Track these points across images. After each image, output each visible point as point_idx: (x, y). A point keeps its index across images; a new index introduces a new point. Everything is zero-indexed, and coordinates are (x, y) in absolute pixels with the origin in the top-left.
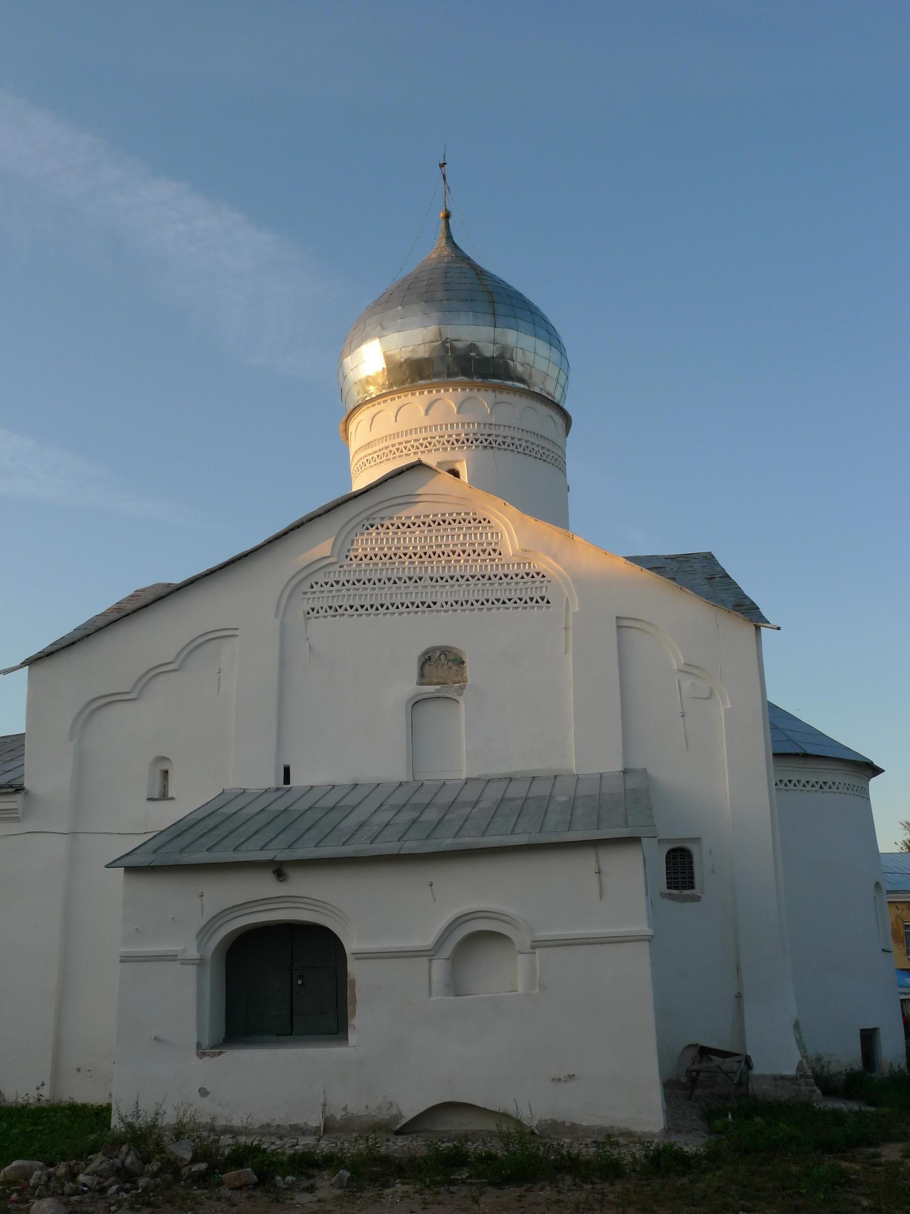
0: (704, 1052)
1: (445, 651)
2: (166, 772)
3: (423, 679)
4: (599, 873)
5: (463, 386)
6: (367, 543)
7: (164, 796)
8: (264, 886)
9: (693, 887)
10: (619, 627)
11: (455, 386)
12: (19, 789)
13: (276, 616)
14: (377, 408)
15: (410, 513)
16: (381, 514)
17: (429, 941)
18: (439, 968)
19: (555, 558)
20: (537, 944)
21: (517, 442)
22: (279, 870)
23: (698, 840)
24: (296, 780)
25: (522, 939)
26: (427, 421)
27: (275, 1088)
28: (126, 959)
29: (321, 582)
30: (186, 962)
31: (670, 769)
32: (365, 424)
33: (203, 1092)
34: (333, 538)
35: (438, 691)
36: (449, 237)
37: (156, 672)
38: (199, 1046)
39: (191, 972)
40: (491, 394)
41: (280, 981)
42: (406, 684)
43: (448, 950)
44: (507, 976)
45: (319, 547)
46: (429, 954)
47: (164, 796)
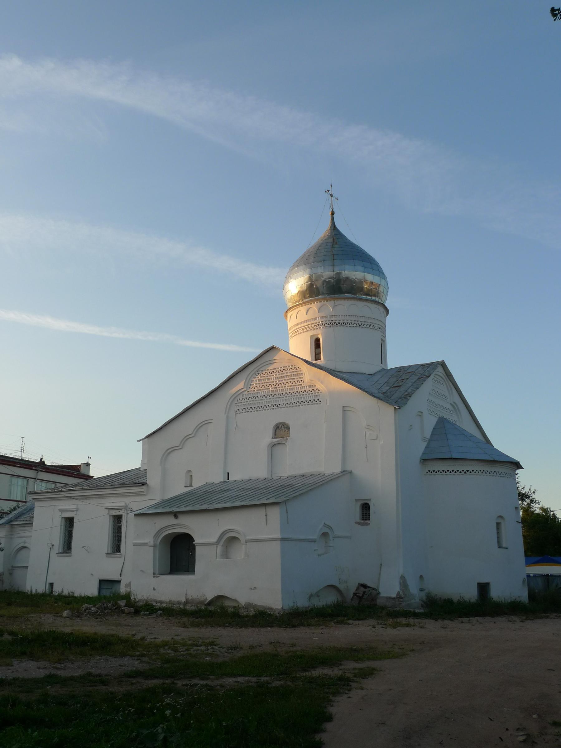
0: (364, 586)
1: (283, 424)
2: (192, 476)
3: (275, 436)
4: (266, 515)
5: (320, 300)
6: (258, 382)
7: (191, 486)
8: (171, 520)
9: (369, 520)
10: (344, 411)
11: (317, 301)
12: (144, 484)
13: (225, 413)
14: (299, 309)
15: (272, 367)
16: (261, 369)
17: (214, 539)
18: (219, 548)
19: (322, 383)
20: (247, 541)
21: (346, 322)
22: (176, 515)
23: (370, 500)
24: (231, 479)
25: (243, 539)
26: (307, 318)
27: (173, 589)
28: (135, 545)
29: (241, 399)
30: (150, 546)
31: (360, 470)
32: (294, 315)
33: (154, 589)
34: (244, 381)
35: (279, 441)
36: (333, 219)
37: (186, 438)
38: (154, 574)
39: (152, 549)
40: (332, 302)
41: (179, 553)
42: (268, 438)
43: (221, 543)
44: (239, 553)
45: (239, 385)
46: (216, 544)
47: (191, 486)
